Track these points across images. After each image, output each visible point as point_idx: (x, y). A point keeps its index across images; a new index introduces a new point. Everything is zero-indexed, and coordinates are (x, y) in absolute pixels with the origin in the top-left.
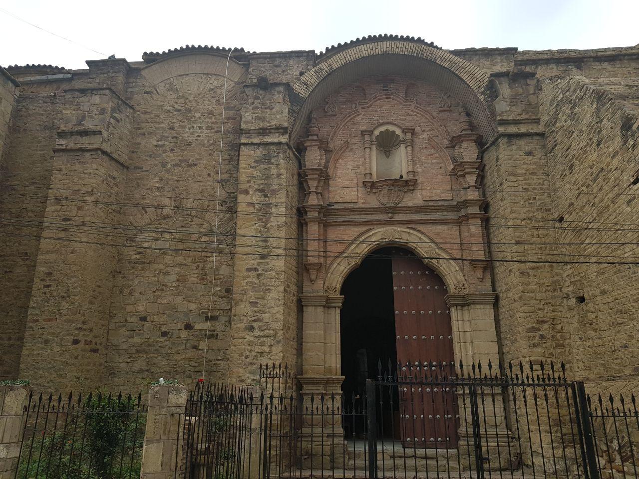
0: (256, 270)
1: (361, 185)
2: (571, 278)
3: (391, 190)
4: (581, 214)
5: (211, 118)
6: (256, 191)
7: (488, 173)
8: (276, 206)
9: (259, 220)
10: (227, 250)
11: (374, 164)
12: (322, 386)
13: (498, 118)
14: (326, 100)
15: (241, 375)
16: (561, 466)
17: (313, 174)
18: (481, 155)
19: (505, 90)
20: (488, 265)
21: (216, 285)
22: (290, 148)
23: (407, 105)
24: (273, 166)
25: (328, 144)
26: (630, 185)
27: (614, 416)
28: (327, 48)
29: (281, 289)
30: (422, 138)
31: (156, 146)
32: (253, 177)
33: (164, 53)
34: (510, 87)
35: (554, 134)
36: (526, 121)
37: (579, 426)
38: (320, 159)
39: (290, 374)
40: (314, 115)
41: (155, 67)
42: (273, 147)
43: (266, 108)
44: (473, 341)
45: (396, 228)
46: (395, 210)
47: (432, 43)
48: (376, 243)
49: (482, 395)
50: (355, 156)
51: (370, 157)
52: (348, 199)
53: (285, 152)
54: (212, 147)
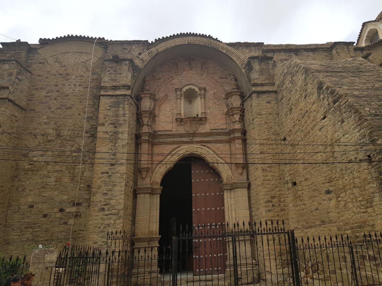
1: (174, 120)
2: (289, 172)
3: (192, 123)
4: (295, 136)
5: (82, 79)
6: (109, 124)
7: (246, 114)
9: (111, 142)
10: (89, 161)
11: (183, 108)
12: (147, 242)
13: (252, 82)
14: (155, 70)
16: (281, 279)
17: (145, 114)
18: (242, 103)
19: (256, 66)
20: (245, 166)
21: (81, 183)
22: (132, 98)
23: (202, 74)
24: (121, 109)
25: (155, 96)
26: (321, 120)
27: (309, 248)
31: (46, 96)
32: (108, 115)
35: (282, 91)
36: (268, 84)
37: (291, 255)
38: (150, 105)
39: (126, 236)
40: (147, 78)
43: (117, 74)
44: (236, 210)
45: (194, 146)
46: (194, 135)
48: (181, 155)
49: (239, 241)
50: (171, 103)
52: (166, 129)
53: (128, 100)
54: (82, 97)
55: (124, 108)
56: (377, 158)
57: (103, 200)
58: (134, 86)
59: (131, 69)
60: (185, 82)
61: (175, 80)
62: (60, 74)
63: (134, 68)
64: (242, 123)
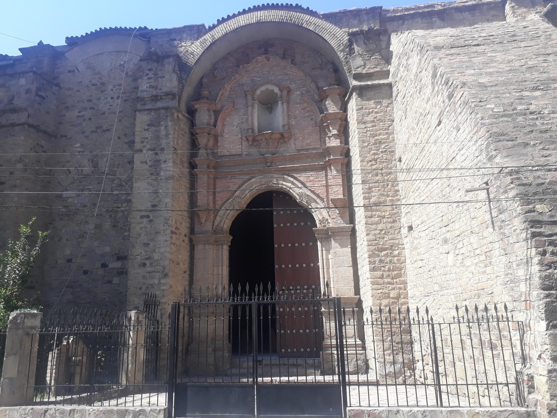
0: (148, 217)
1: (244, 139)
6: (148, 150)
8: (165, 162)
9: (151, 174)
15: (136, 303)
22: (179, 111)
28: (218, 20)
29: (168, 232)
30: (296, 95)
31: (78, 116)
32: (147, 138)
33: (82, 36)
34: (365, 43)
40: (205, 80)
47: (308, 8)
51: (252, 115)
52: (234, 152)
53: (172, 115)
55: (166, 127)
56: (495, 186)
58: (181, 94)
59: (178, 69)
61: (245, 78)
62: (93, 85)
63: (182, 67)
64: (343, 138)
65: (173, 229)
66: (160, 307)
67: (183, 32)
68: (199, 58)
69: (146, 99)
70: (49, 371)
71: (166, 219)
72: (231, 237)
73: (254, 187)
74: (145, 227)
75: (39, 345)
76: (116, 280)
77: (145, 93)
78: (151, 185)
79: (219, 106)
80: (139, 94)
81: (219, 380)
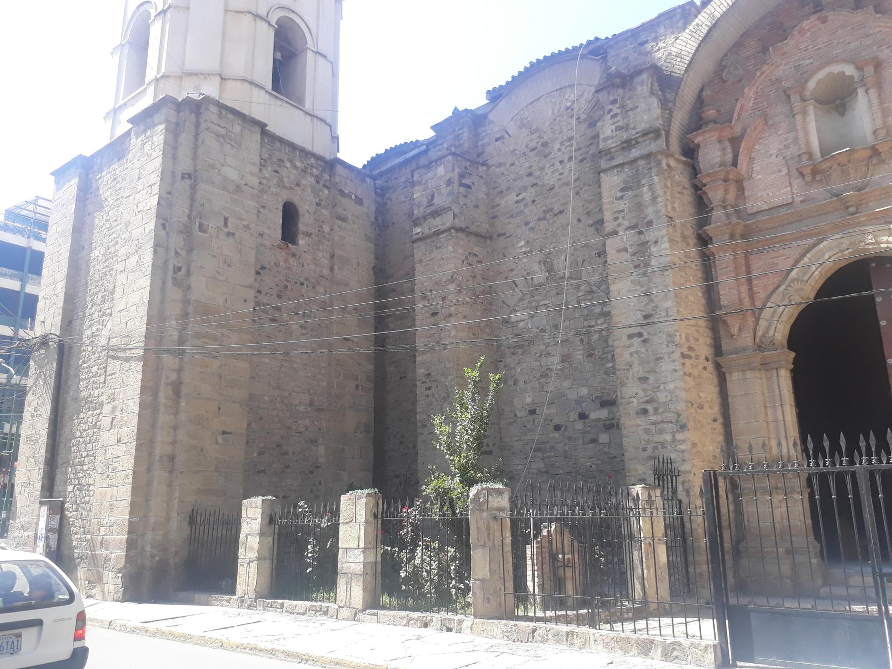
0: (640, 335)
1: (794, 173)
6: (626, 229)
8: (656, 242)
9: (636, 267)
14: (724, 63)
15: (640, 472)
22: (668, 156)
24: (645, 189)
29: (677, 355)
31: (517, 202)
32: (623, 211)
33: (507, 83)
40: (707, 93)
41: (502, 104)
42: (642, 163)
52: (776, 201)
53: (659, 163)
55: (651, 186)
57: (641, 393)
59: (658, 88)
60: (812, 63)
62: (532, 150)
63: (665, 83)
65: (685, 350)
66: (680, 479)
67: (658, 25)
68: (692, 58)
69: (613, 150)
70: (529, 573)
71: (669, 336)
72: (793, 355)
73: (827, 257)
74: (637, 352)
75: (512, 535)
76: (604, 438)
77: (610, 141)
78: (639, 283)
79: (738, 130)
80: (602, 145)
81: (807, 605)
